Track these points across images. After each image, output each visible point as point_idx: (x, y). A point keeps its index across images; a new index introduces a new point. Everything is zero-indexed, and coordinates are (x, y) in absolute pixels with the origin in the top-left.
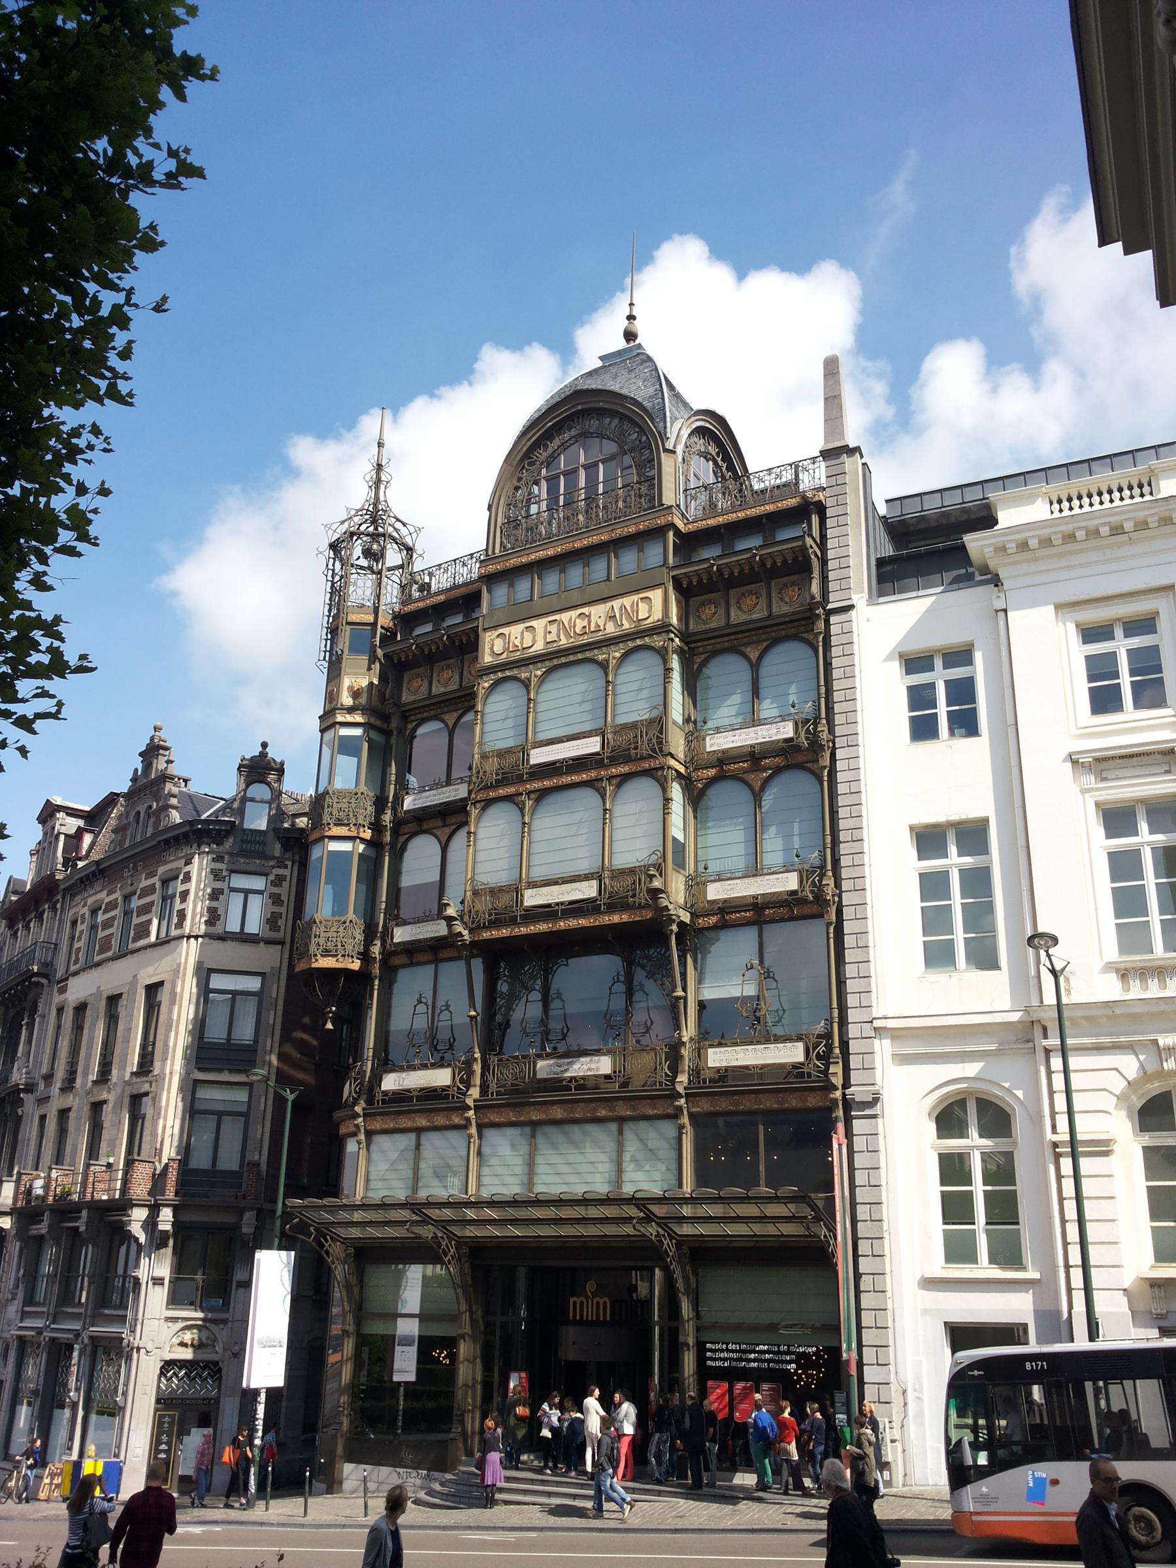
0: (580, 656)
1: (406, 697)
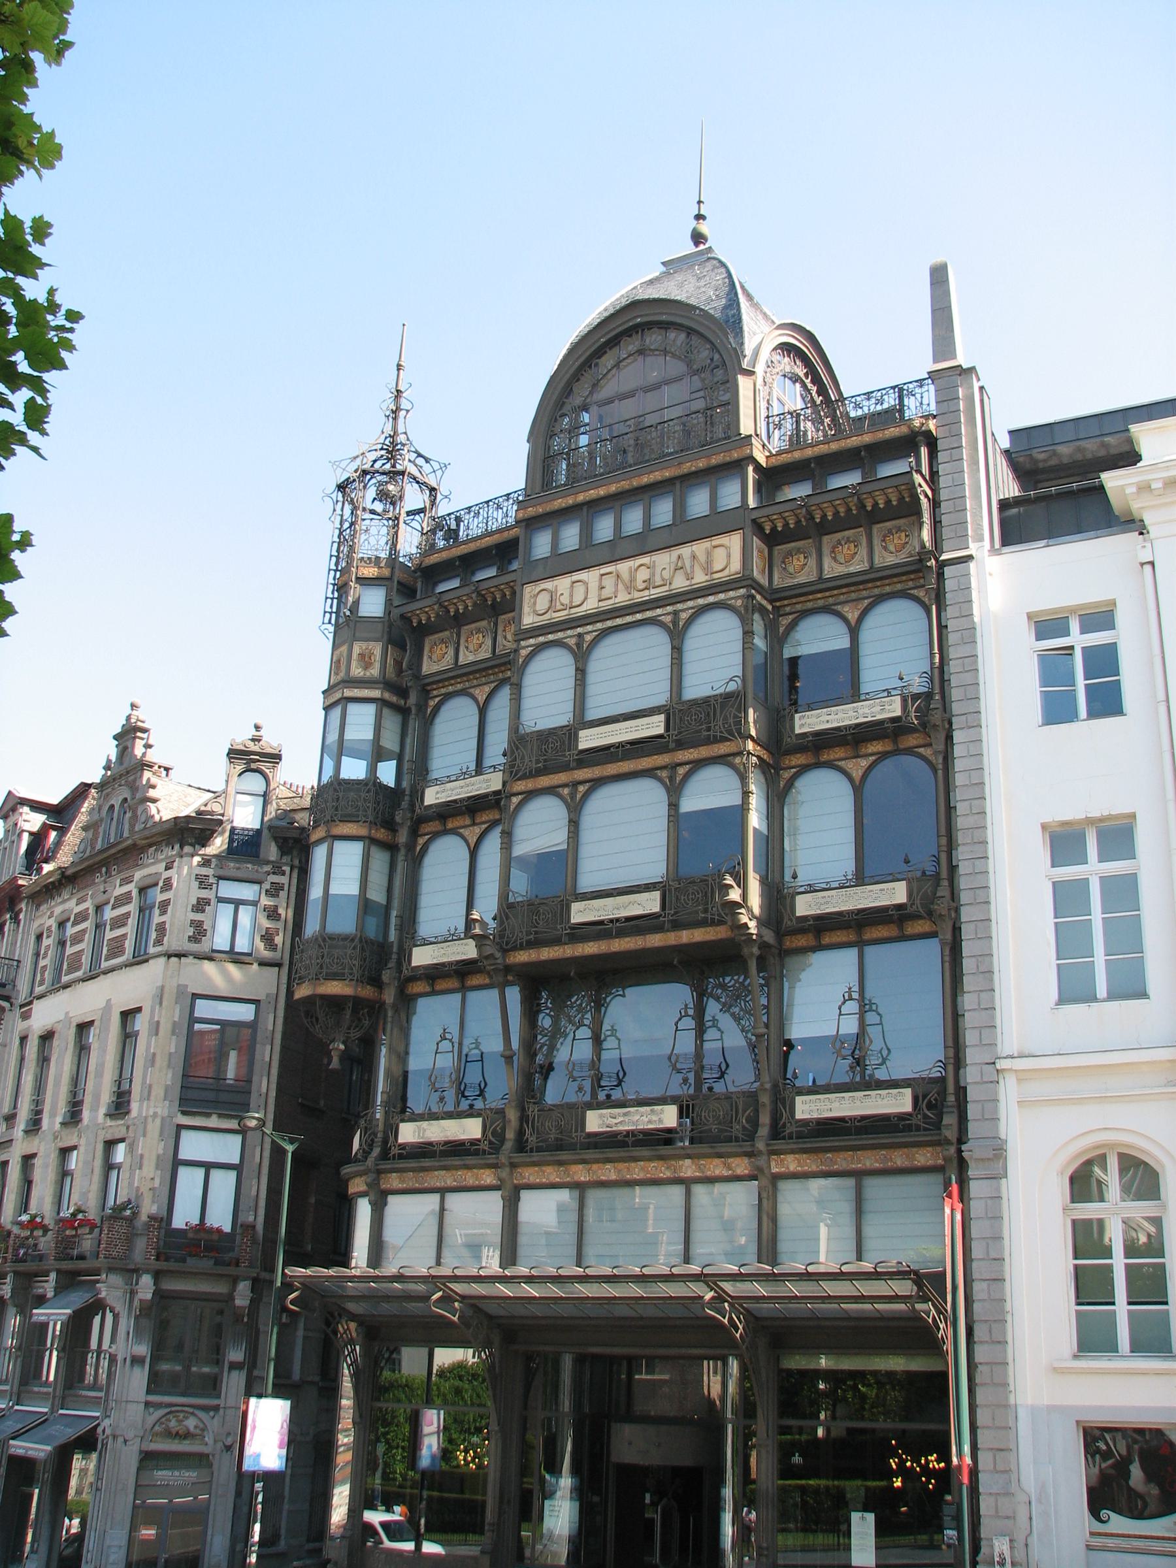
0: (639, 616)
1: (429, 667)
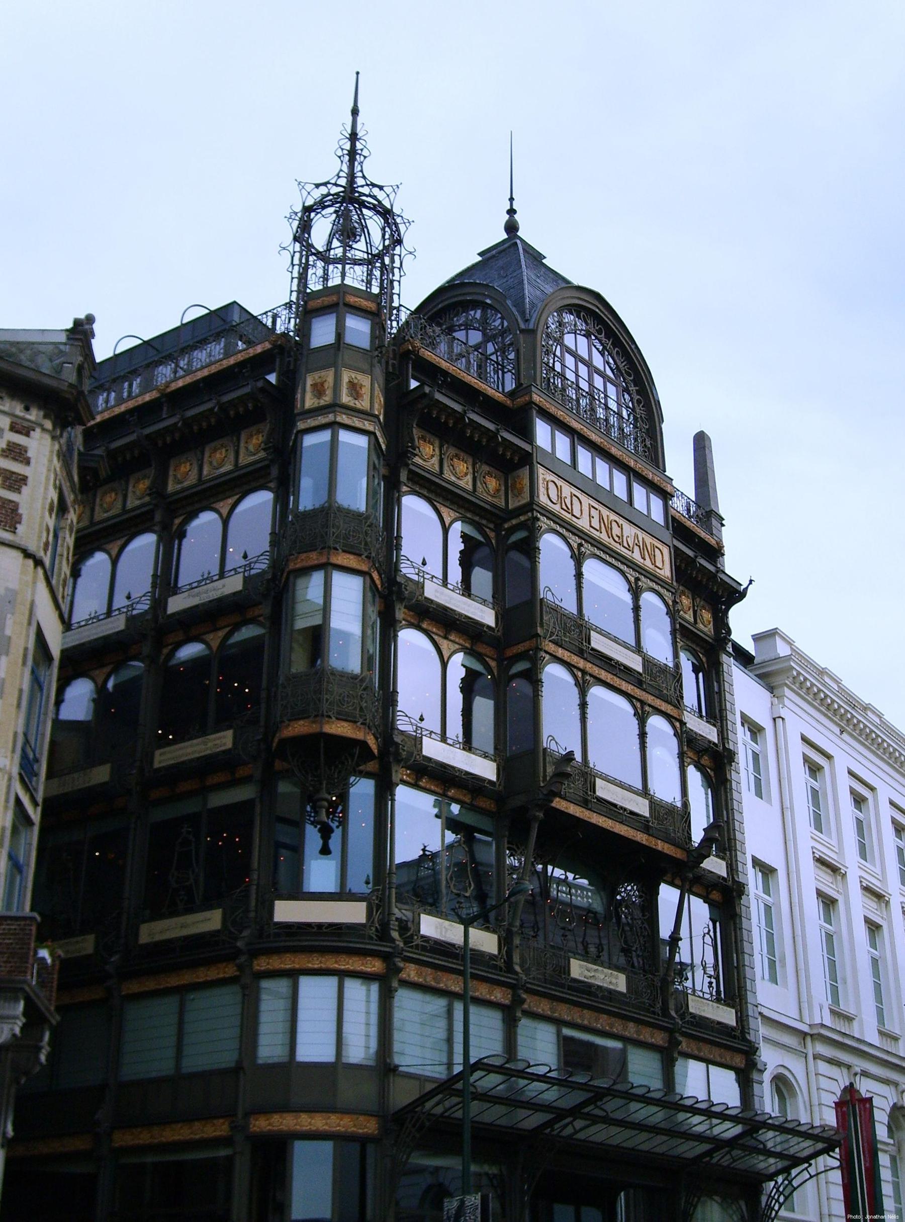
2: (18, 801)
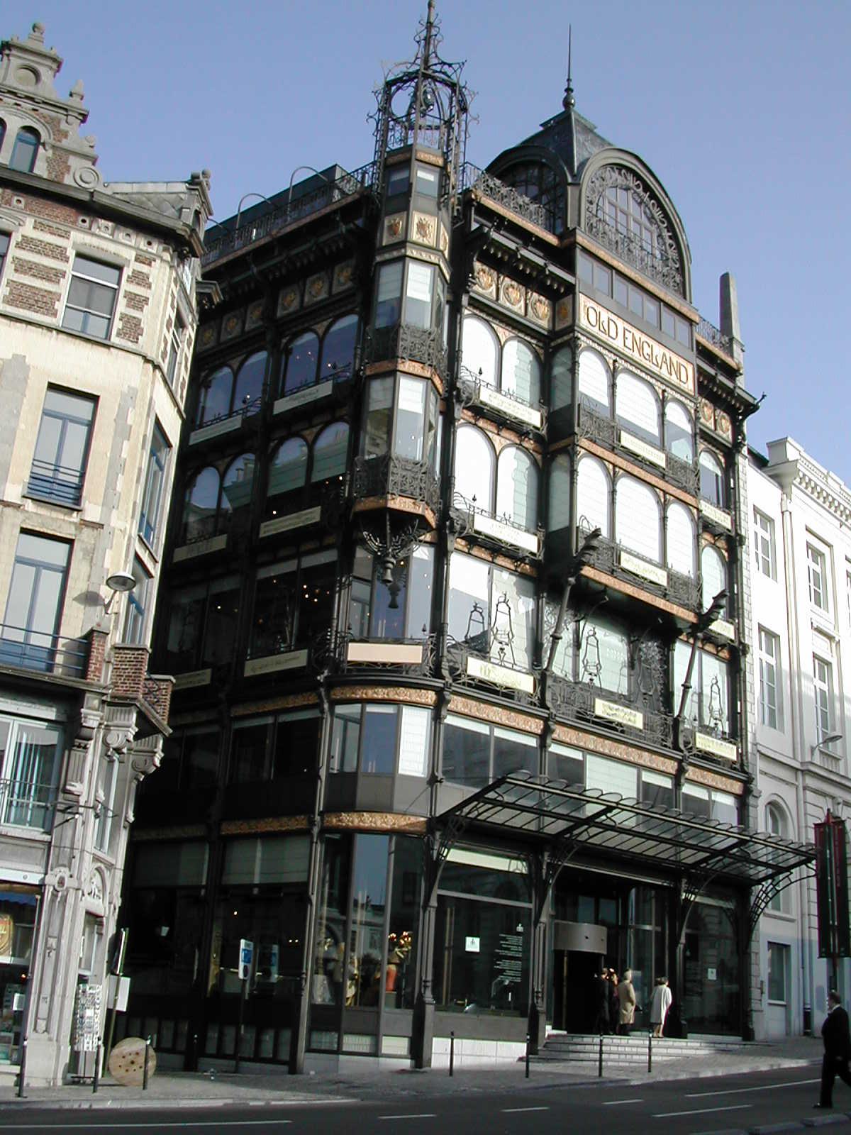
0: (643, 375)
2: (137, 557)
